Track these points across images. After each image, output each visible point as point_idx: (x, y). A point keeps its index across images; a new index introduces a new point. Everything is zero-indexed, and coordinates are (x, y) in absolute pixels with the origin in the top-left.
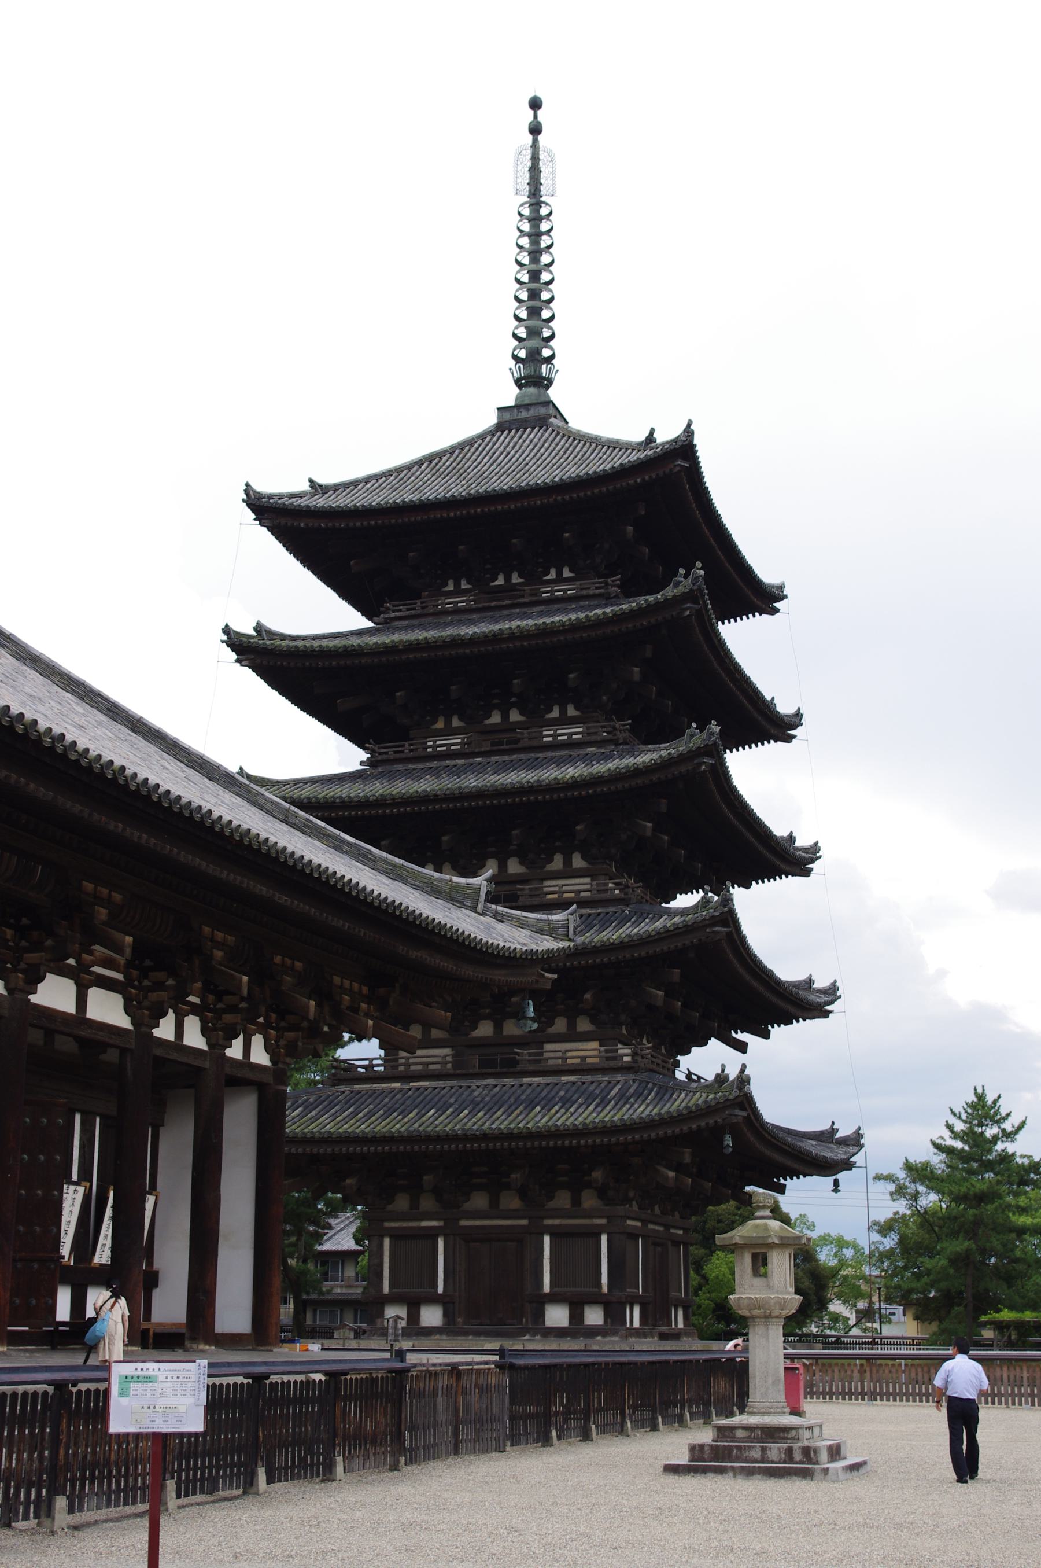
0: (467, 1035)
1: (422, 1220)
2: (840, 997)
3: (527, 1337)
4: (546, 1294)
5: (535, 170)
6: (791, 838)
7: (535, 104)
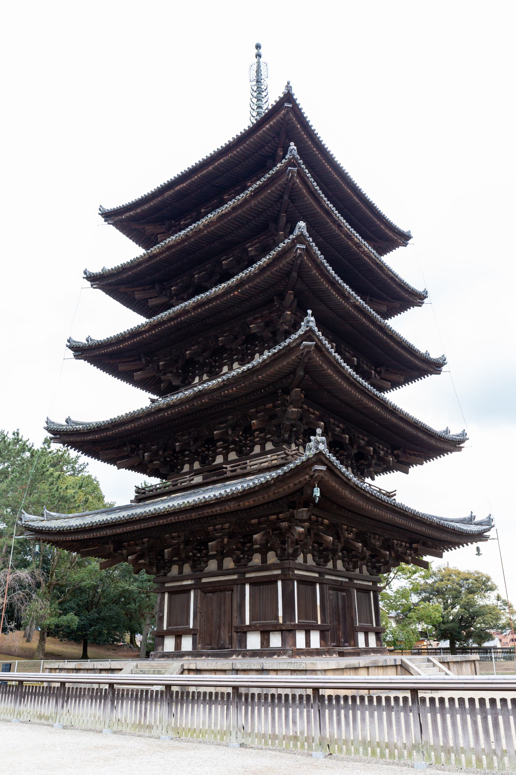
0: (210, 464)
1: (183, 580)
4: (248, 626)
5: (258, 72)
7: (258, 47)
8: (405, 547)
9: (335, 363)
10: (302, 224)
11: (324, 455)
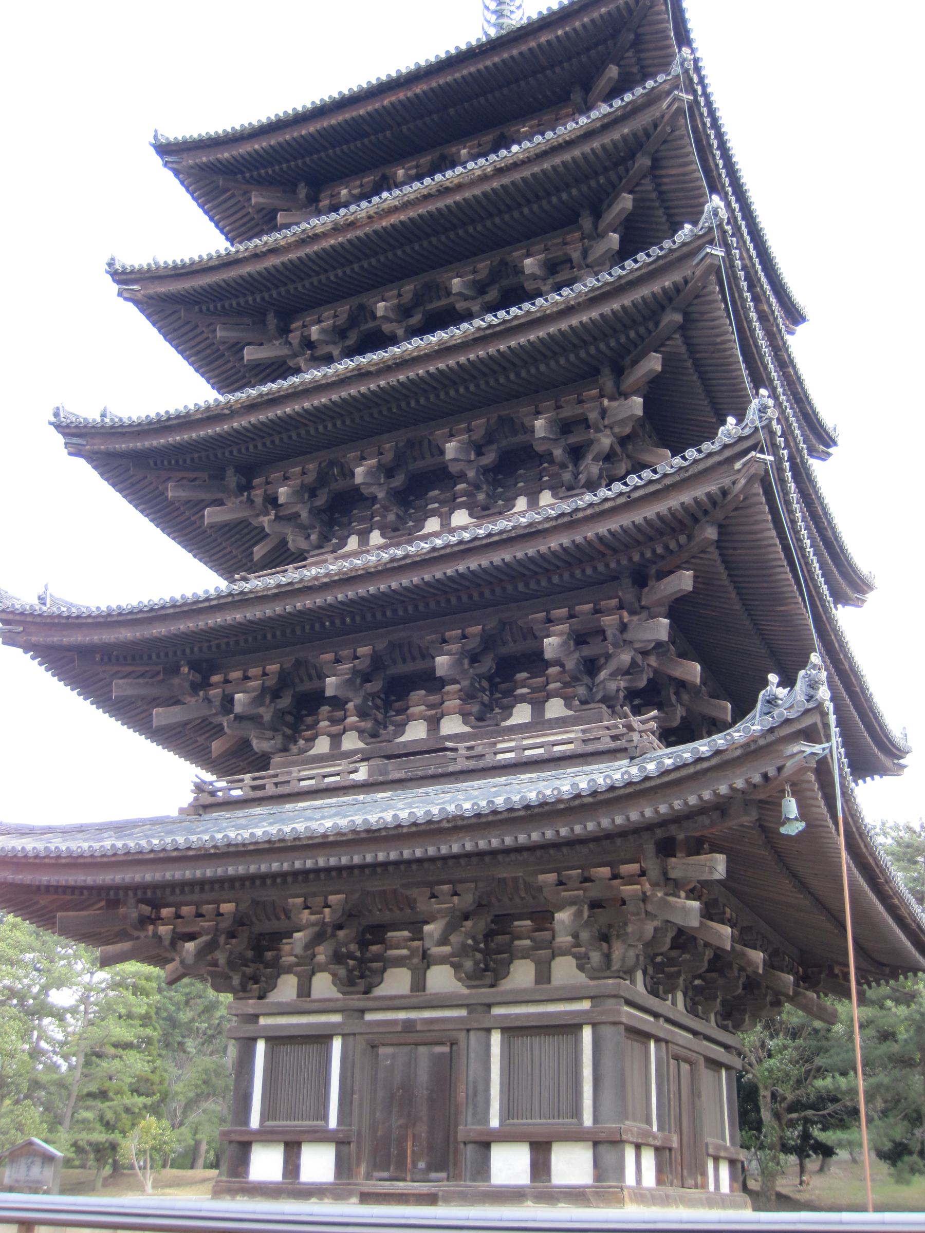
8: (615, 876)
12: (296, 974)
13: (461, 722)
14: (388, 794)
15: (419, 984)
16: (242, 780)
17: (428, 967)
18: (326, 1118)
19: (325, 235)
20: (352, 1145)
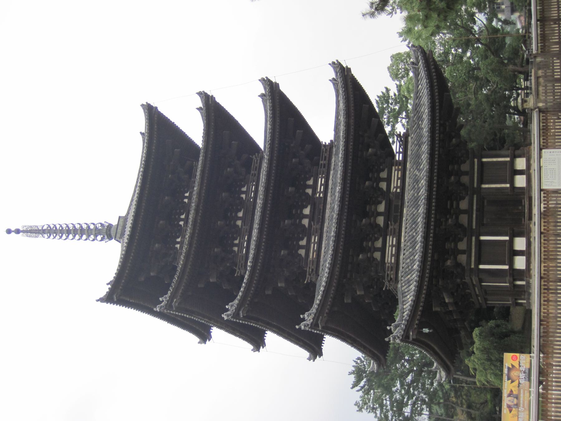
2: (337, 61)
3: (531, 291)
6: (262, 96)
7: (9, 231)
9: (325, 291)
10: (224, 316)
11: (402, 336)
12: (458, 255)
13: (380, 205)
14: (405, 209)
15: (464, 212)
16: (388, 267)
17: (460, 208)
18: (505, 241)
19: (196, 217)
20: (515, 229)
